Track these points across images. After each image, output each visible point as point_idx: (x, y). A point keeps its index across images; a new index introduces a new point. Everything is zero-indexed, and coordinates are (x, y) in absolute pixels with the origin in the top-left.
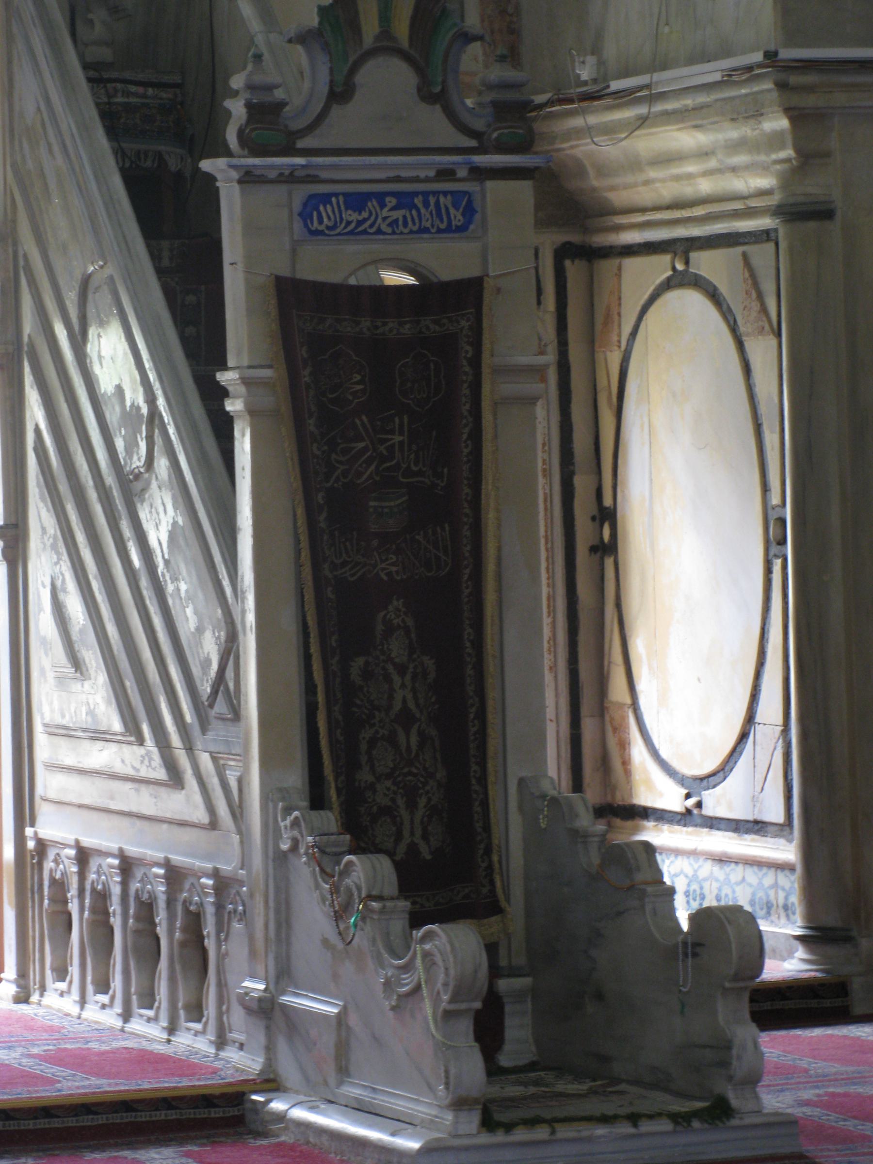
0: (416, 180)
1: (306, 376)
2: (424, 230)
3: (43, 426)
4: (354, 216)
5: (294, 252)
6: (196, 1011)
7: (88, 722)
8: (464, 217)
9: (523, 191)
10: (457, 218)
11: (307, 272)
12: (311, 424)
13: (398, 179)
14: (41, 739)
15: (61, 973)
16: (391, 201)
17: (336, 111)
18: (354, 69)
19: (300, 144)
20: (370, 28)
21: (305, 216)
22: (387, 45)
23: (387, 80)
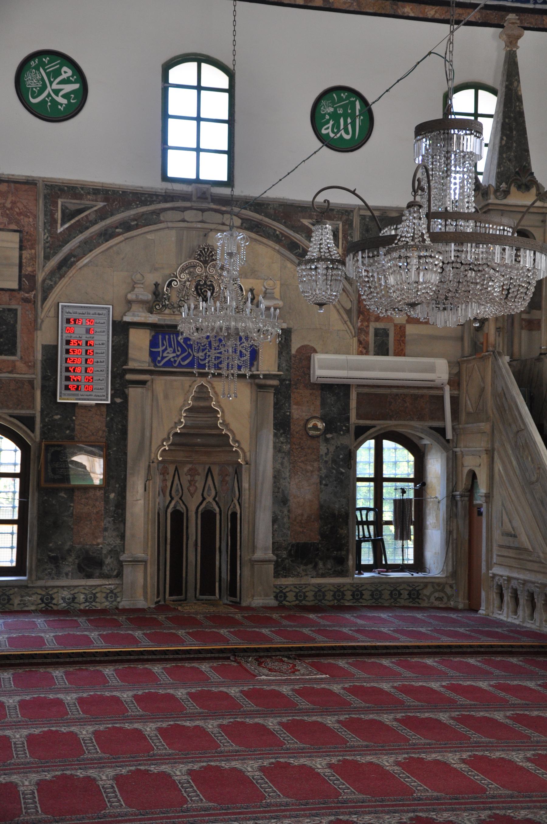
14: (495, 548)
15: (501, 608)
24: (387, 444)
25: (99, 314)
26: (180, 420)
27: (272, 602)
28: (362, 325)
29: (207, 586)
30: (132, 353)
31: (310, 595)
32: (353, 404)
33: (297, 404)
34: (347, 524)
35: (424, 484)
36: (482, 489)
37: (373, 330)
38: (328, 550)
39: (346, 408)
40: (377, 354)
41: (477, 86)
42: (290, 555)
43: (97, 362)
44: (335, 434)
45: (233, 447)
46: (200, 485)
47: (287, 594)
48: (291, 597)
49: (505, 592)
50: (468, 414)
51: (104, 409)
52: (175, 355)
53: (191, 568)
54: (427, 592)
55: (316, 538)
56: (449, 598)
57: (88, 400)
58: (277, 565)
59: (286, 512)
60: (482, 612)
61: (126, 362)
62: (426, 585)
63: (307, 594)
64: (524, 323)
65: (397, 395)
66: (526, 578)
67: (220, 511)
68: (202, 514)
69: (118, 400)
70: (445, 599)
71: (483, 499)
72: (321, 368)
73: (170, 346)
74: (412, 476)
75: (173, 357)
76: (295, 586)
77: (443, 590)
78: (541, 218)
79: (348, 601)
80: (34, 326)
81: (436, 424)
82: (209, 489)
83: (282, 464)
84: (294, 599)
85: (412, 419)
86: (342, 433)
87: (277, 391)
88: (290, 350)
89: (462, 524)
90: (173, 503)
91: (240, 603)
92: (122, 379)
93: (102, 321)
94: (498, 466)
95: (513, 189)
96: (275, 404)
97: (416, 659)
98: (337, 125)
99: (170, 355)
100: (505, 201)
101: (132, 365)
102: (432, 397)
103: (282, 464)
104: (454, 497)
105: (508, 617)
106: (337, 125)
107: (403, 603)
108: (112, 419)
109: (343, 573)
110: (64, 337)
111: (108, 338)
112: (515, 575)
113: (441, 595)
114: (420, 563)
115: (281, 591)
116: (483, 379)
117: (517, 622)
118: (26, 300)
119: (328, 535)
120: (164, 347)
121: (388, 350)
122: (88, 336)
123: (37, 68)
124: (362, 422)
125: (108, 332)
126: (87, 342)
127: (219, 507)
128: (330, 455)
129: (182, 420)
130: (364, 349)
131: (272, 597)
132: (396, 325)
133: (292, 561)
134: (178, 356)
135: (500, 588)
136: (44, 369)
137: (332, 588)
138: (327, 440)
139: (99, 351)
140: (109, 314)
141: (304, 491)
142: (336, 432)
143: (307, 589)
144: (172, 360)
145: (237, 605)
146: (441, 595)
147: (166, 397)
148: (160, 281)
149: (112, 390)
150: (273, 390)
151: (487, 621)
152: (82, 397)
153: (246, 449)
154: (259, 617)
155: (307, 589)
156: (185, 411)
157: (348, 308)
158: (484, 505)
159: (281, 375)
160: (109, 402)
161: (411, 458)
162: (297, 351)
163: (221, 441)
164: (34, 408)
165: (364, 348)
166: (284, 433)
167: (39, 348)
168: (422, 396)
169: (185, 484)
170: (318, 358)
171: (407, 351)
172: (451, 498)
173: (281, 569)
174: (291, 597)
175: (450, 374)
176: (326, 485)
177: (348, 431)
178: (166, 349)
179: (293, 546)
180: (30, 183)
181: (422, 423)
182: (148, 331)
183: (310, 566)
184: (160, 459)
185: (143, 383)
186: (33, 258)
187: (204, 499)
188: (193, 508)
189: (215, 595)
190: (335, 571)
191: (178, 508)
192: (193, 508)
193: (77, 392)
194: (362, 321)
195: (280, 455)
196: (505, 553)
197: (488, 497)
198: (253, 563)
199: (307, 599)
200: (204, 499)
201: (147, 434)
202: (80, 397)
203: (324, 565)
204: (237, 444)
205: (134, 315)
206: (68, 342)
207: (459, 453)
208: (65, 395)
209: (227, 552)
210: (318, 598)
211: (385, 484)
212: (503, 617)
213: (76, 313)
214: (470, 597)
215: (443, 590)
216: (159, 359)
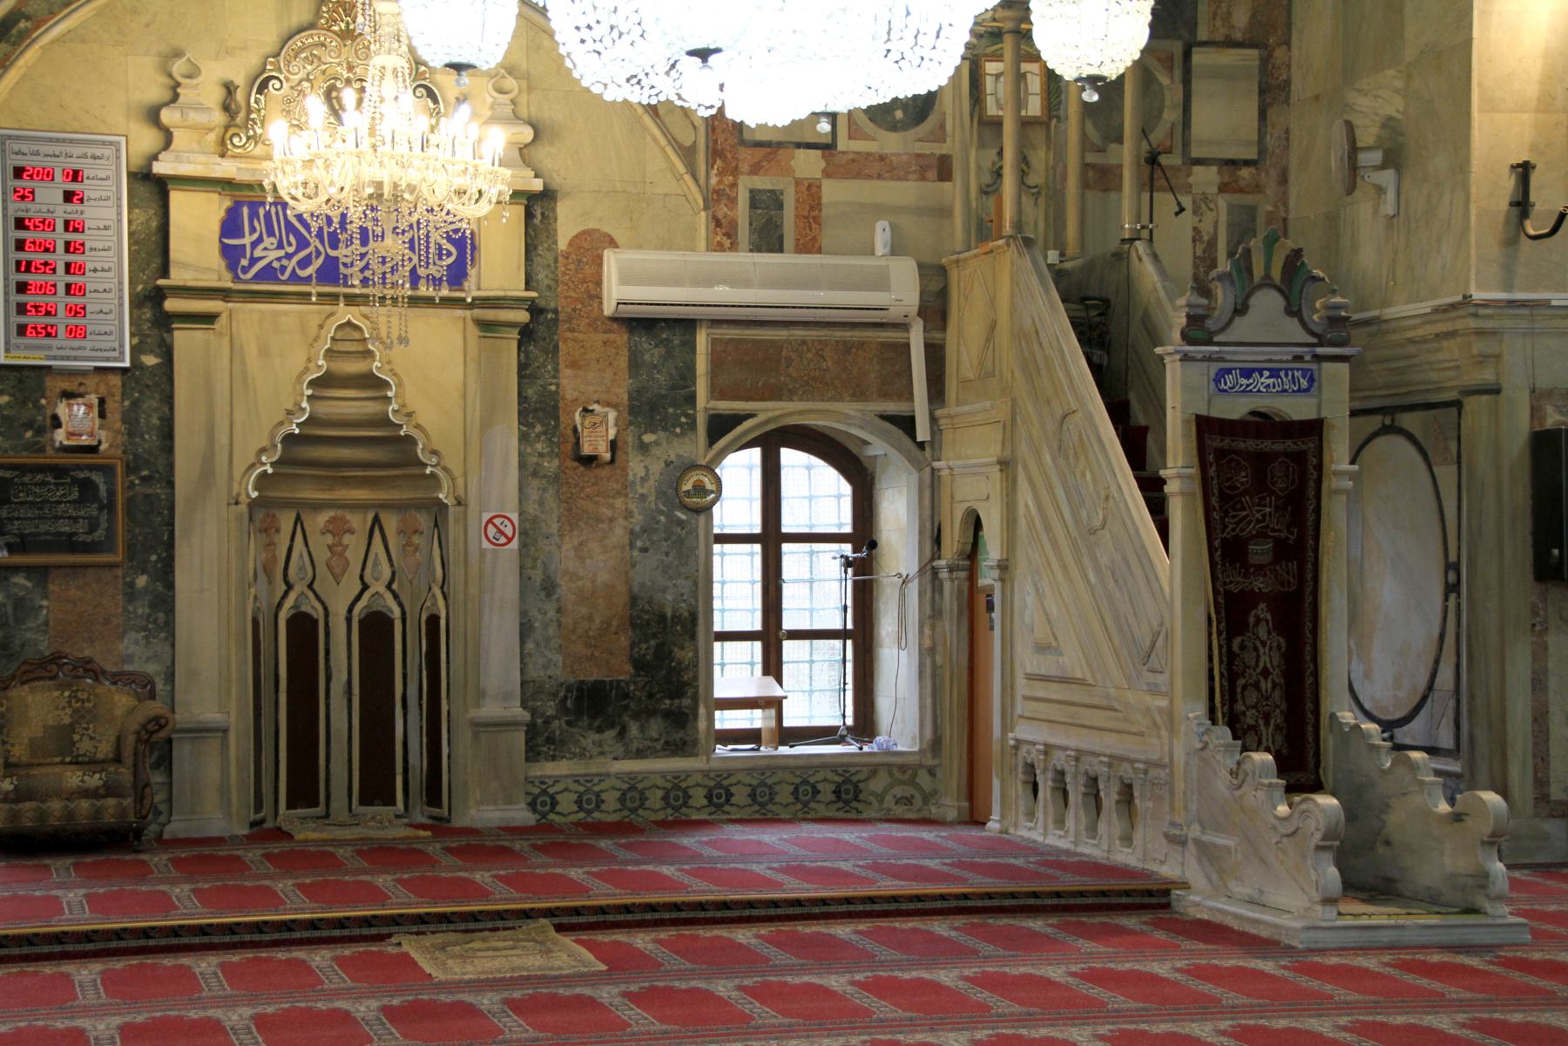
0: (1281, 361)
1: (1212, 471)
2: (1285, 391)
3: (1030, 503)
4: (1244, 381)
5: (1209, 401)
6: (1127, 839)
7: (1059, 673)
9: (1343, 369)
10: (1304, 383)
11: (1215, 414)
12: (1214, 501)
13: (1271, 361)
14: (1020, 681)
15: (1031, 815)
16: (1267, 373)
17: (1238, 320)
18: (1248, 296)
19: (1216, 339)
20: (1258, 272)
21: (1217, 381)
22: (1267, 282)
23: (1267, 303)
24: (790, 458)
25: (94, 157)
26: (298, 405)
27: (521, 815)
28: (720, 182)
29: (376, 787)
30: (179, 248)
31: (611, 800)
33: (574, 365)
34: (693, 637)
35: (873, 545)
36: (992, 550)
37: (747, 195)
38: (650, 696)
39: (687, 374)
40: (756, 248)
42: (562, 707)
43: (95, 270)
44: (661, 434)
45: (425, 465)
46: (354, 555)
47: (559, 798)
48: (566, 803)
49: (1040, 779)
50: (965, 382)
51: (116, 381)
52: (281, 253)
53: (339, 748)
54: (876, 785)
55: (623, 671)
56: (926, 799)
57: (76, 359)
58: (532, 731)
59: (552, 614)
60: (993, 825)
61: (165, 271)
62: (874, 769)
63: (603, 796)
64: (1091, 173)
65: (804, 342)
66: (1084, 746)
67: (403, 613)
68: (361, 622)
69: (150, 360)
70: (918, 802)
71: (996, 573)
72: (624, 281)
73: (271, 233)
74: (848, 529)
75: (279, 259)
77: (912, 782)
79: (698, 809)
82: (375, 565)
83: (541, 503)
84: (575, 808)
85: (838, 398)
86: (678, 430)
87: (526, 334)
88: (555, 243)
89: (950, 628)
90: (292, 596)
91: (449, 821)
92: (156, 310)
93: (102, 174)
94: (1025, 496)
96: (522, 367)
97: (815, 929)
99: (269, 253)
101: (177, 277)
102: (887, 346)
103: (541, 503)
104: (935, 572)
105: (1045, 835)
107: (822, 810)
108: (135, 404)
109: (683, 747)
110: (10, 212)
111: (119, 214)
112: (1054, 740)
113: (909, 791)
114: (865, 724)
115: (544, 792)
116: (992, 301)
117: (1064, 844)
119: (650, 667)
120: (256, 236)
121: (781, 239)
122: (69, 207)
125: (119, 199)
126: (67, 223)
127: (401, 605)
128: (652, 482)
129: (305, 404)
130: (724, 234)
131: (523, 805)
132: (798, 183)
133: (569, 723)
134: (289, 256)
135: (1030, 768)
137: (660, 782)
138: (644, 448)
139: (100, 245)
140: (118, 158)
141: (595, 563)
142: (664, 429)
143: (603, 786)
144: (276, 265)
145: (440, 827)
146: (909, 791)
147: (264, 352)
148: (240, 80)
149: (132, 335)
150: (514, 334)
151: (1003, 844)
152: (61, 353)
153: (457, 471)
154: (481, 847)
155: (603, 786)
156: (312, 384)
157: (688, 143)
158: (997, 586)
159: (533, 300)
160: (127, 364)
161: (846, 488)
162: (570, 244)
165: (728, 235)
166: (545, 433)
168: (862, 344)
169: (322, 555)
170: (611, 260)
171: (826, 240)
172: (929, 572)
173: (540, 741)
174: (566, 803)
175: (922, 293)
176: (644, 550)
177: (692, 425)
178: (260, 240)
179: (569, 689)
181: (860, 406)
182: (215, 196)
183: (610, 734)
184: (255, 494)
185: (210, 318)
187: (365, 587)
188: (339, 609)
189: (393, 802)
190: (667, 742)
191: (303, 609)
192: (339, 609)
193: (47, 341)
194: (720, 174)
195: (535, 483)
196: (1040, 690)
197: (1004, 567)
198: (480, 726)
199: (603, 807)
200: (365, 587)
201: (222, 438)
202: (55, 352)
203: (642, 729)
204: (434, 460)
205: (178, 160)
206: (20, 224)
207: (945, 473)
208: (18, 347)
209: (420, 706)
210: (629, 804)
211: (786, 547)
212: (1036, 836)
213: (37, 154)
214: (971, 797)
215: (912, 782)
216: (244, 262)
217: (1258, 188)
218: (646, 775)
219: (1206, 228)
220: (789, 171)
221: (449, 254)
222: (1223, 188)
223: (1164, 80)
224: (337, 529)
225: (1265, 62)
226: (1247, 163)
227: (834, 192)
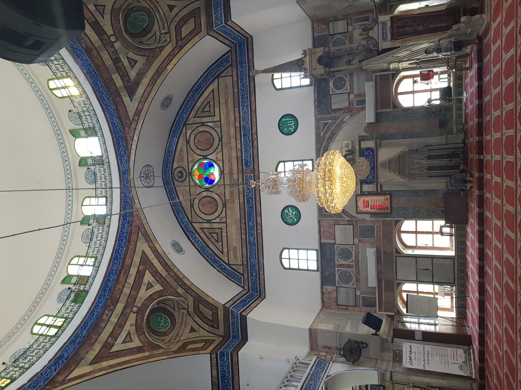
8: (384, 24)
22: (368, 34)
23: (371, 34)
24: (399, 91)
30: (371, 190)
32: (385, 110)
41: (273, 79)
76: (456, 126)
78: (312, 54)
80: (364, 220)
81: (391, 76)
87: (381, 139)
95: (304, 67)
98: (291, 127)
100: (308, 69)
101: (375, 190)
106: (291, 127)
118: (356, 223)
123: (287, 219)
124: (392, 106)
130: (364, 109)
136: (378, 217)
163: (400, 157)
164: (391, 221)
167: (371, 219)
180: (319, 222)
185: (381, 186)
186: (342, 221)
188: (427, 163)
192: (427, 163)
217: (351, 18)
218: (456, 114)
219: (358, 27)
220: (353, 99)
221: (369, 152)
222: (352, 25)
223: (335, 38)
224: (413, 164)
225: (331, 21)
226: (347, 21)
227: (356, 92)
